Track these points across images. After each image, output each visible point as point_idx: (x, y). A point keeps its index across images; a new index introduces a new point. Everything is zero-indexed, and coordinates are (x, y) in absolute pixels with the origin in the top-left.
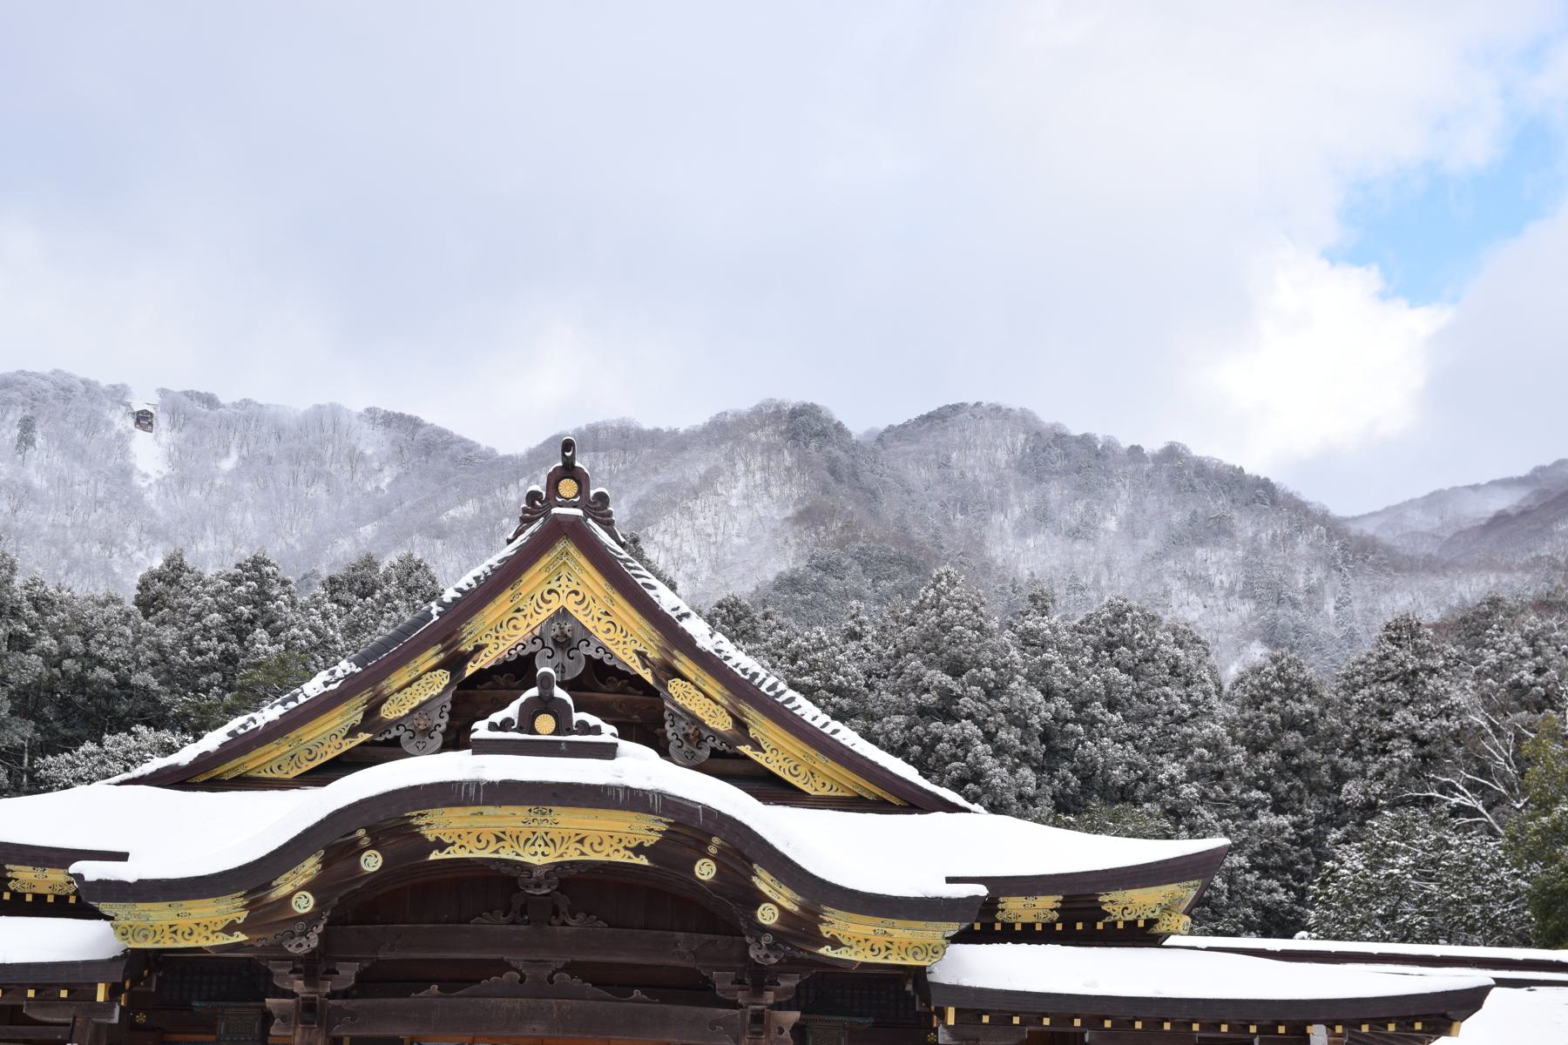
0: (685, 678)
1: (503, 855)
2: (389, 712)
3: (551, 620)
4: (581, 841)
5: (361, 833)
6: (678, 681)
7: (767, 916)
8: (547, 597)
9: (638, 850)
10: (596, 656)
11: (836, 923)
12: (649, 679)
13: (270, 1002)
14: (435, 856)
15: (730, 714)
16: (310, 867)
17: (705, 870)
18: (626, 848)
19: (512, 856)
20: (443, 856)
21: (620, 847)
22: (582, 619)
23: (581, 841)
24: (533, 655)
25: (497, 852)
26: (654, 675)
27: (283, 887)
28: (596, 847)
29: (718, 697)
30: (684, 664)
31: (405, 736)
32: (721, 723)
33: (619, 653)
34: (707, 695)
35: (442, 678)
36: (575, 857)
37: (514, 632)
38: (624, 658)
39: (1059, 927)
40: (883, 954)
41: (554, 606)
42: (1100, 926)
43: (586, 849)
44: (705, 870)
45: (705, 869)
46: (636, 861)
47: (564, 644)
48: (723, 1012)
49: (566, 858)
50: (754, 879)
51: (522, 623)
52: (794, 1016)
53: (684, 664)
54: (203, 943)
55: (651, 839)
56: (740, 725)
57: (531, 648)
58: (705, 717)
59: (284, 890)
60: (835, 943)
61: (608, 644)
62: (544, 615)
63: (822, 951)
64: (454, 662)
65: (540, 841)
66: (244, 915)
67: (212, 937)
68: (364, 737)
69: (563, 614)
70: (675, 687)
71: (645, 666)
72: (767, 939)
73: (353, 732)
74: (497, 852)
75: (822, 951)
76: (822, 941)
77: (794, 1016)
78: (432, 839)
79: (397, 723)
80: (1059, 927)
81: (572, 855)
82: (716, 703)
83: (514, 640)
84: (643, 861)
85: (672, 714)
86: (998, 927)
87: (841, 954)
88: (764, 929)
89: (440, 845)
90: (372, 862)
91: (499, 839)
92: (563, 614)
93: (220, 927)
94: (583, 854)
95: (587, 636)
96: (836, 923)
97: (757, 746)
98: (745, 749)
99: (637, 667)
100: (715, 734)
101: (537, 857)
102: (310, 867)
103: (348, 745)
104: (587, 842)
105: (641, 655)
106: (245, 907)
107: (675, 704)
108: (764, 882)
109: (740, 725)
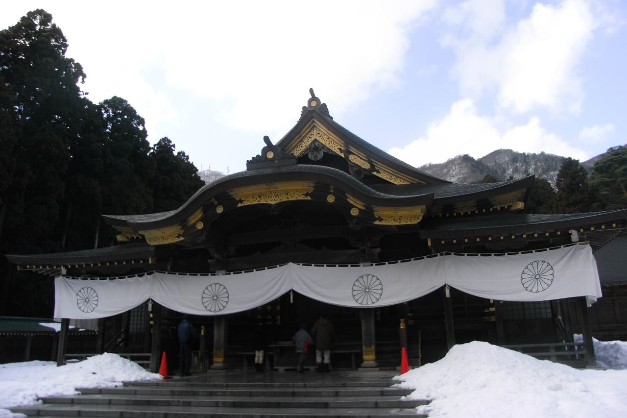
0: (354, 154)
1: (262, 202)
3: (312, 143)
4: (287, 194)
5: (213, 199)
6: (352, 155)
7: (354, 212)
8: (310, 136)
9: (307, 195)
10: (326, 151)
11: (379, 211)
12: (342, 155)
13: (209, 261)
14: (239, 205)
15: (369, 163)
16: (199, 214)
17: (331, 199)
18: (303, 195)
19: (265, 202)
20: (242, 205)
21: (300, 194)
22: (321, 141)
23: (287, 194)
24: (307, 154)
25: (259, 201)
26: (344, 155)
27: (192, 220)
28: (292, 195)
29: (364, 158)
30: (352, 149)
32: (366, 166)
33: (333, 150)
34: (361, 158)
36: (286, 200)
37: (301, 148)
38: (335, 151)
39: (477, 212)
40: (399, 221)
41: (313, 139)
42: (491, 210)
43: (289, 196)
44: (331, 199)
45: (331, 198)
46: (306, 198)
48: (352, 251)
49: (282, 201)
50: (348, 199)
51: (304, 145)
52: (378, 250)
53: (352, 149)
54: (172, 242)
55: (311, 190)
56: (373, 166)
57: (307, 152)
58: (361, 165)
59: (193, 221)
60: (380, 219)
61: (329, 147)
63: (376, 223)
65: (273, 196)
66: (183, 231)
67: (174, 239)
69: (316, 140)
70: (351, 157)
71: (341, 152)
74: (259, 201)
75: (376, 223)
76: (376, 219)
77: (378, 250)
78: (238, 200)
80: (477, 212)
81: (285, 199)
82: (365, 160)
83: (301, 151)
84: (309, 198)
85: (351, 165)
86: (455, 214)
87: (383, 223)
89: (241, 201)
90: (220, 210)
91: (260, 197)
92: (316, 140)
93: (176, 236)
94: (288, 198)
95: (324, 146)
96: (379, 211)
97: (378, 172)
98: (375, 173)
99: (339, 153)
100: (365, 170)
101: (272, 201)
102: (199, 214)
104: (289, 194)
105: (340, 149)
106: (182, 229)
107: (352, 162)
108: (351, 200)
109: (373, 166)
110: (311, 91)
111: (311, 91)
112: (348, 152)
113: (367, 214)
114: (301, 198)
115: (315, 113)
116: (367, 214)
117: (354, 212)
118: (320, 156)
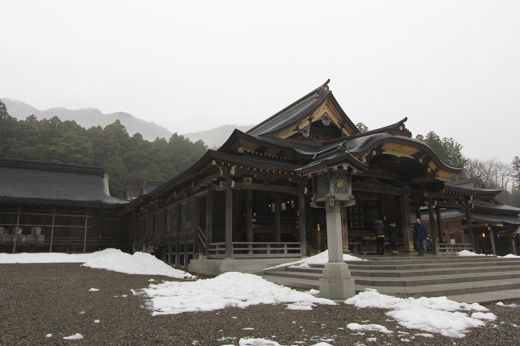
2: (301, 127)
12: (339, 127)
14: (384, 153)
30: (347, 126)
31: (303, 133)
35: (308, 122)
44: (421, 161)
47: (326, 118)
62: (323, 113)
64: (310, 120)
68: (296, 132)
70: (344, 130)
72: (430, 175)
73: (294, 131)
79: (302, 130)
84: (413, 158)
88: (429, 173)
95: (330, 118)
103: (294, 133)
110: (329, 81)
111: (329, 81)
112: (342, 126)
113: (434, 173)
114: (410, 157)
115: (323, 95)
116: (434, 173)
117: (429, 170)
118: (328, 124)
